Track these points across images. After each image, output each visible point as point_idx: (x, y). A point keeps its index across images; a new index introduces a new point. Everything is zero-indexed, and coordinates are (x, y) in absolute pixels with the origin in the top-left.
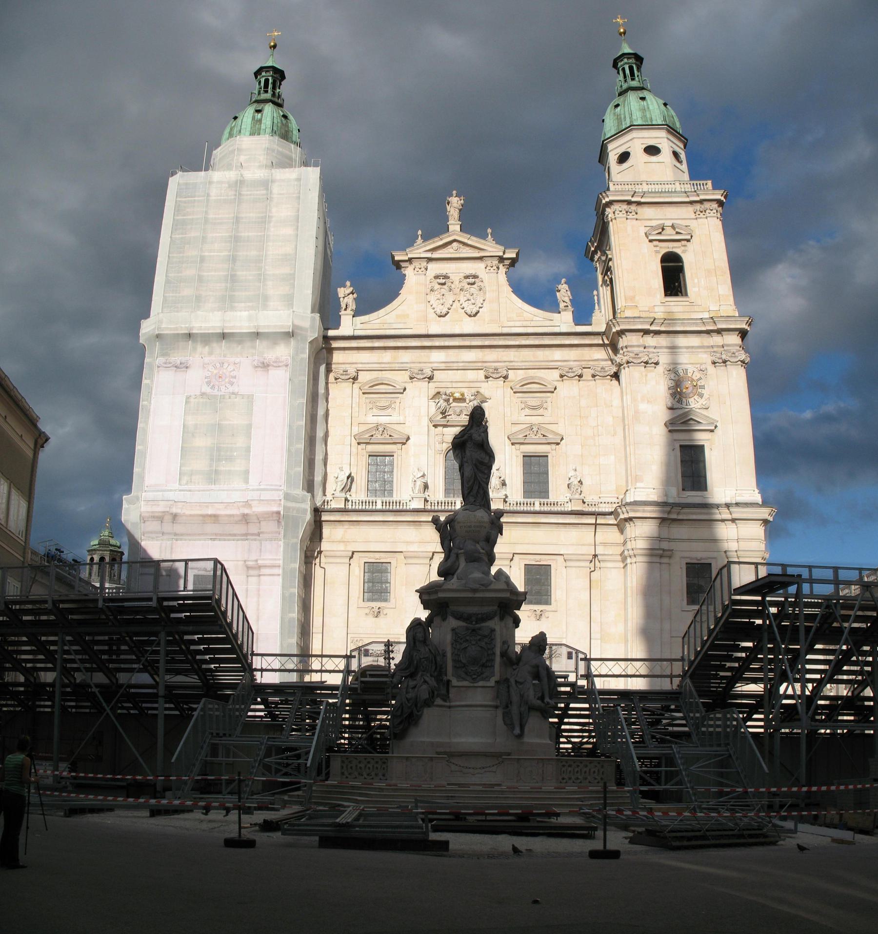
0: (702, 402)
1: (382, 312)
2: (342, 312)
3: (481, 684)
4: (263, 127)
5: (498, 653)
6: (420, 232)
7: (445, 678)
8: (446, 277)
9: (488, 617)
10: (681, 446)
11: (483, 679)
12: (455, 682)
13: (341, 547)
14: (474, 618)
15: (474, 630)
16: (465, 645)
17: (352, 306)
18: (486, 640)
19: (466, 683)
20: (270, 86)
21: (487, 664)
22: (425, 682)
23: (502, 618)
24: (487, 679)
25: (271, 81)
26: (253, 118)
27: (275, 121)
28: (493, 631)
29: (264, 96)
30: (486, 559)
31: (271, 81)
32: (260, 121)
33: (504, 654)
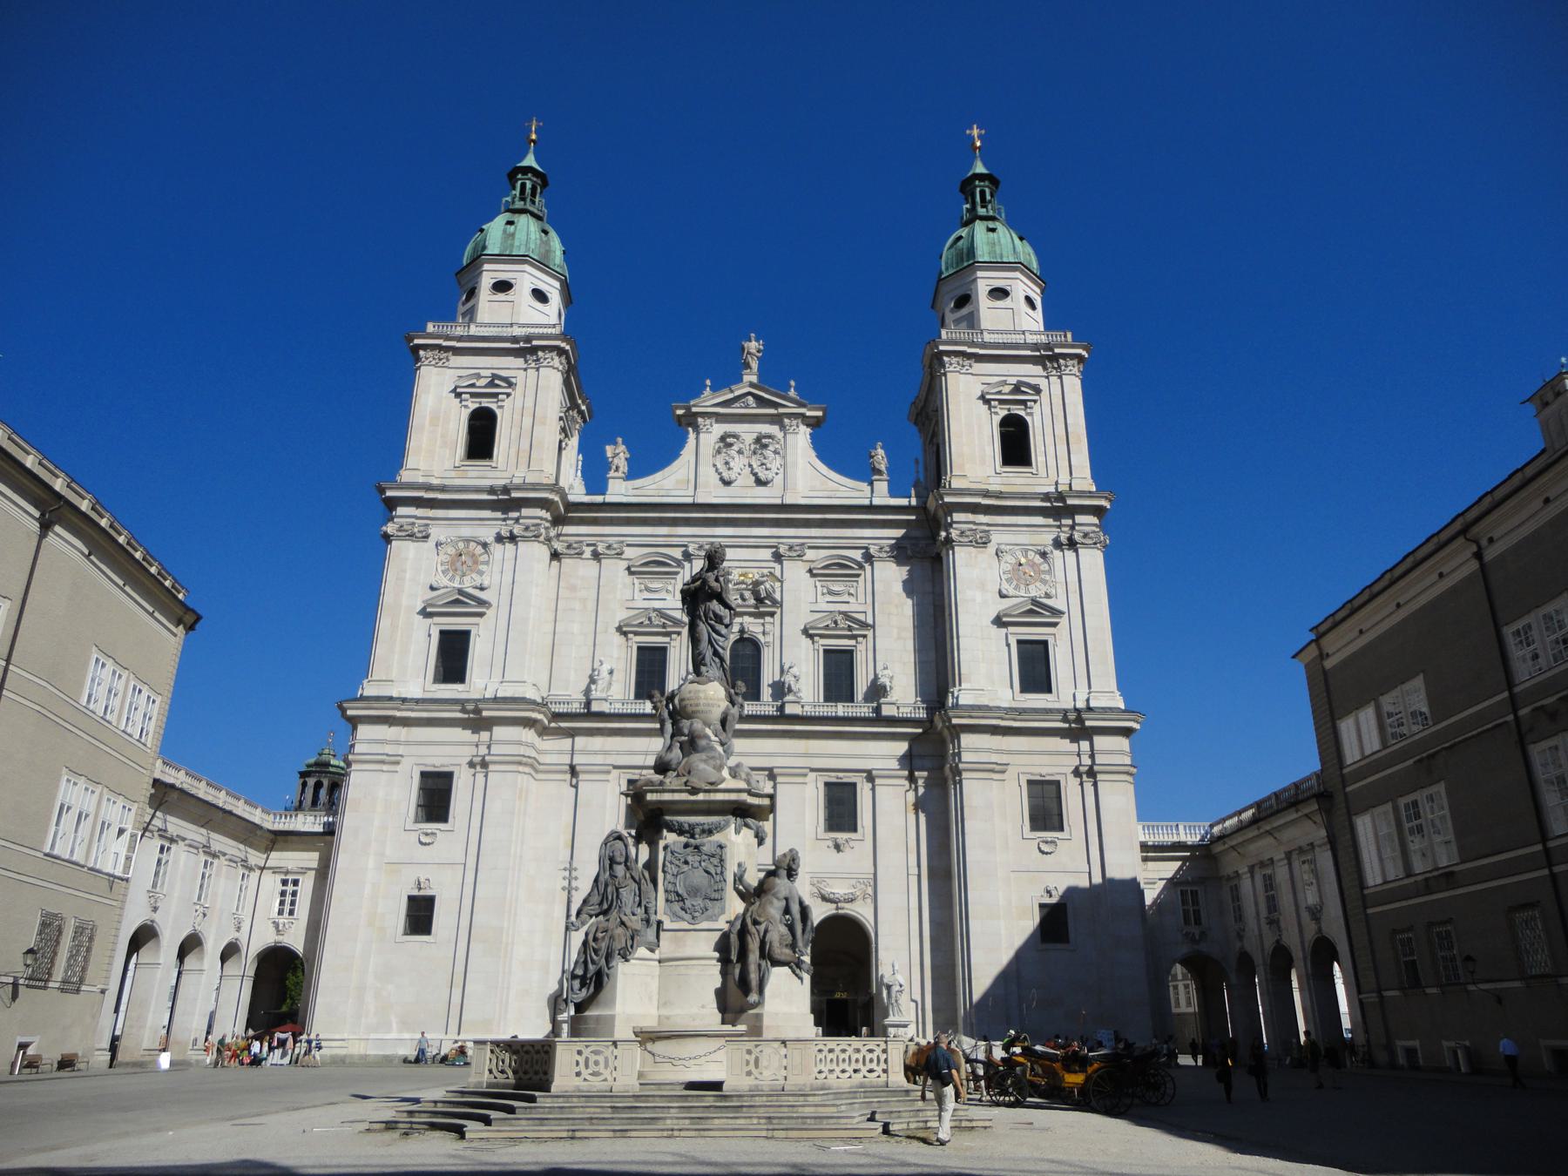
0: (1044, 589)
1: (658, 476)
2: (612, 474)
3: (705, 925)
4: (517, 243)
5: (730, 878)
6: (708, 382)
7: (653, 918)
8: (735, 436)
9: (719, 828)
10: (1019, 642)
11: (710, 919)
12: (667, 924)
13: (599, 759)
14: (697, 830)
15: (697, 847)
16: (686, 868)
17: (624, 467)
18: (715, 861)
19: (685, 925)
20: (528, 191)
21: (716, 897)
22: (623, 923)
23: (737, 832)
24: (714, 918)
25: (529, 185)
26: (505, 231)
27: (533, 236)
28: (721, 847)
29: (519, 205)
30: (720, 749)
31: (529, 185)
32: (513, 235)
33: (739, 879)
